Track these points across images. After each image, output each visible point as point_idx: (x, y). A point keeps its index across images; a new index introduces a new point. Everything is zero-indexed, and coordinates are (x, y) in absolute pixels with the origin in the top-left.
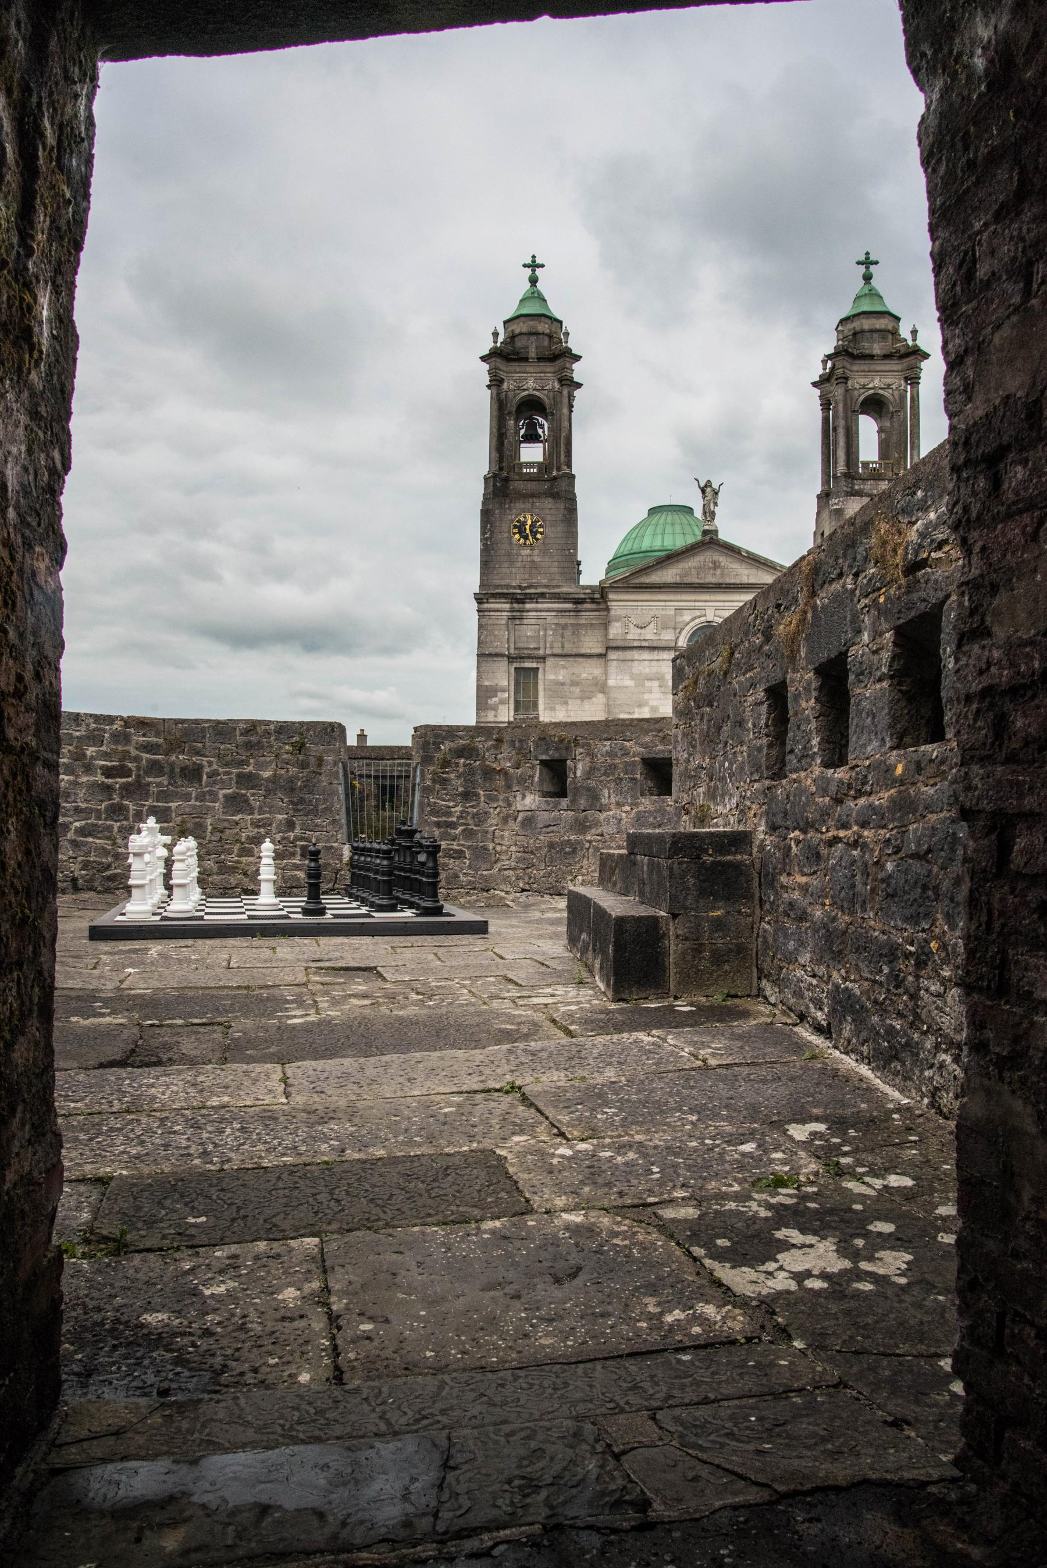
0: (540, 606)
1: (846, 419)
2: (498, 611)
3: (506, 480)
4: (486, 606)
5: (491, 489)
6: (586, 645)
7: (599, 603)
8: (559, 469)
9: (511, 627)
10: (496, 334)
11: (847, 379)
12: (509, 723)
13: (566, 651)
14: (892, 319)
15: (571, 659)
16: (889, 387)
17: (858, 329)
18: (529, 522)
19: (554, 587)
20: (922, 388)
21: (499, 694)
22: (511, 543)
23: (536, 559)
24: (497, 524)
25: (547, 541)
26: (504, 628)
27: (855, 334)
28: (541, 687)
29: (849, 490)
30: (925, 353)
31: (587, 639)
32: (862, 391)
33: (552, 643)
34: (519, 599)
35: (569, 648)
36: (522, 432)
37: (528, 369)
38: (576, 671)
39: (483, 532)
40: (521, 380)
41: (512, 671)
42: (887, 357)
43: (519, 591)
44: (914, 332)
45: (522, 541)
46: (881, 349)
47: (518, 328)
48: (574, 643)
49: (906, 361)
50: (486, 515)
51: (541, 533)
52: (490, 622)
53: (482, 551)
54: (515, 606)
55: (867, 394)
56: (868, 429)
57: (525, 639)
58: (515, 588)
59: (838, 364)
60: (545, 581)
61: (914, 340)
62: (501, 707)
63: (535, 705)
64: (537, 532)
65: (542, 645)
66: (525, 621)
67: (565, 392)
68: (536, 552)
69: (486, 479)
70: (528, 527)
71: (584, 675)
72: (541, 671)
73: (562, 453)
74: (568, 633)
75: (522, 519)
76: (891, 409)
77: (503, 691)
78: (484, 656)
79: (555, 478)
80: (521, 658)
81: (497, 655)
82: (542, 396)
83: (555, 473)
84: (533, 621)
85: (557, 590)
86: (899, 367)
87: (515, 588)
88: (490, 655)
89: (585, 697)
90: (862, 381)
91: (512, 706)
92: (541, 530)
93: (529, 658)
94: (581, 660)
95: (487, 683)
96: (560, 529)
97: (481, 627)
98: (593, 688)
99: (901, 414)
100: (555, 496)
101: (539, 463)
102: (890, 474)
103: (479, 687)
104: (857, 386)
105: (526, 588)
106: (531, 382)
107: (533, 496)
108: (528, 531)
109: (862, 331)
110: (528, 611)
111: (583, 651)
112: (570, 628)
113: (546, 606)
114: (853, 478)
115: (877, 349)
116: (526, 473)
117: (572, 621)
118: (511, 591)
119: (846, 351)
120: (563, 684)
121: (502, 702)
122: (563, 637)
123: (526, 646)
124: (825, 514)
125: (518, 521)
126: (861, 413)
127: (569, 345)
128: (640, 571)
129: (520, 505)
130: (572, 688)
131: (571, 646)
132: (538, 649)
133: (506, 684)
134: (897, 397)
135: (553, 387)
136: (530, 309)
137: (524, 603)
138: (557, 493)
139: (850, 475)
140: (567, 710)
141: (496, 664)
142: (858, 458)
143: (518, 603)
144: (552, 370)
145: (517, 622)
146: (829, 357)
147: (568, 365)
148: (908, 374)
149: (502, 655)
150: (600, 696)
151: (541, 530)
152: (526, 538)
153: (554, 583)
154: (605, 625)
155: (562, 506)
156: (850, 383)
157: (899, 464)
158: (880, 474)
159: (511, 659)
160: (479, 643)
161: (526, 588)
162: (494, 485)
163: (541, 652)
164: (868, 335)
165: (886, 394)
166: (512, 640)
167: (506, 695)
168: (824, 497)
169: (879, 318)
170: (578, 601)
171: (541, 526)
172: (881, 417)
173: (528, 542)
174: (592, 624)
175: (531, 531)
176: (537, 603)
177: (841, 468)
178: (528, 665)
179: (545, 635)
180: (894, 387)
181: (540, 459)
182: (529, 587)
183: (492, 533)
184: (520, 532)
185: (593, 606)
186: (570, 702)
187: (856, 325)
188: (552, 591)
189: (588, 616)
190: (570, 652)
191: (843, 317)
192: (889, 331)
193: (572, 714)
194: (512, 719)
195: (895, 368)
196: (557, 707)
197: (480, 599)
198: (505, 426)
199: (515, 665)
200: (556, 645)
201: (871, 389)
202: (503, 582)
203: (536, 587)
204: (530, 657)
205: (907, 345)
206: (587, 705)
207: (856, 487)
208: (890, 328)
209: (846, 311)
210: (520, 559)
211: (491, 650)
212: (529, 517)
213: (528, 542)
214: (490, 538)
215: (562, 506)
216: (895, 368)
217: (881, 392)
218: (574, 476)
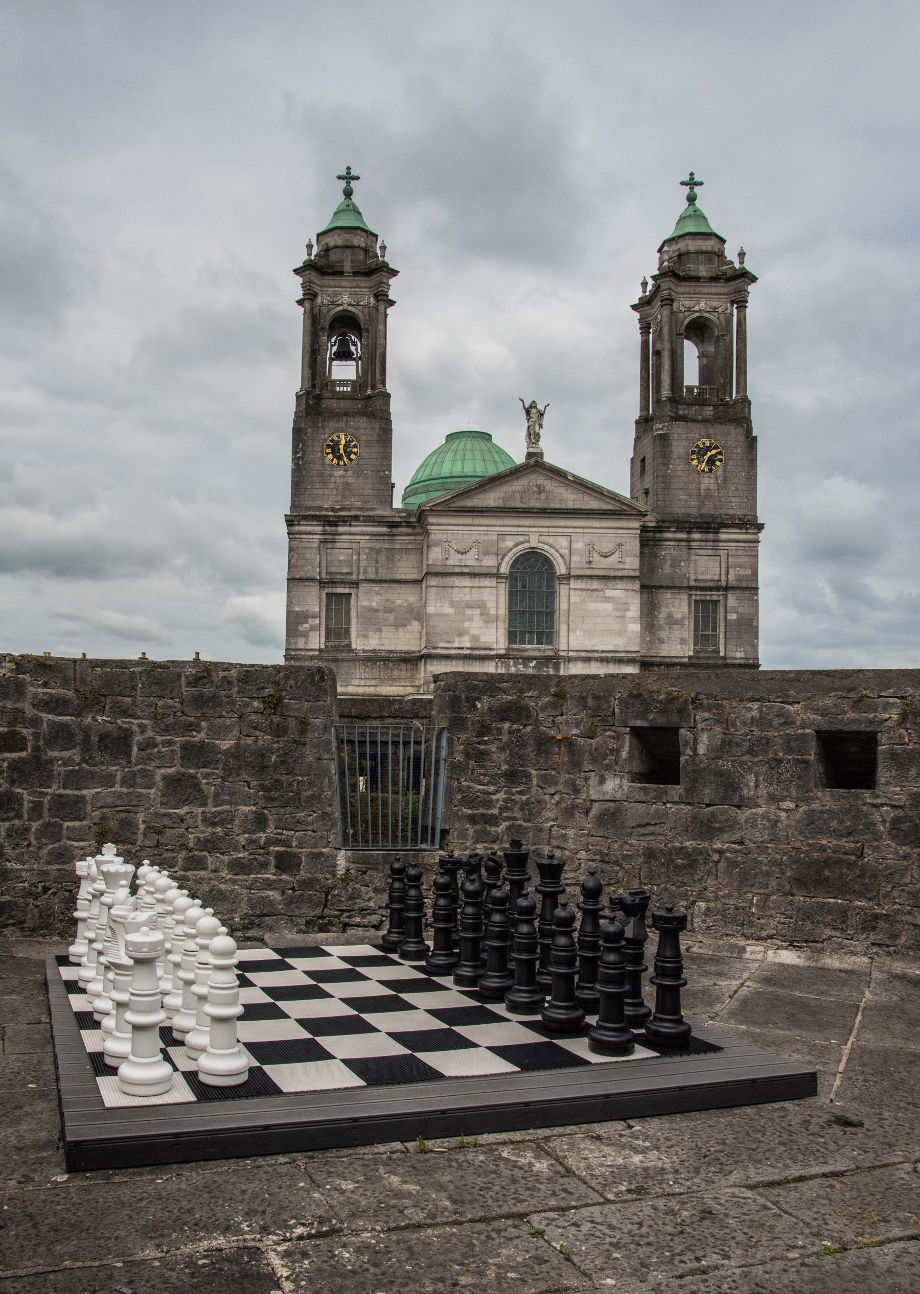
0: (353, 529)
1: (671, 342)
2: (310, 533)
3: (319, 398)
4: (297, 528)
5: (304, 406)
6: (401, 570)
7: (414, 527)
8: (373, 387)
9: (323, 551)
10: (310, 247)
11: (672, 300)
12: (320, 650)
13: (379, 577)
14: (717, 240)
15: (385, 585)
16: (715, 309)
17: (683, 250)
18: (343, 442)
19: (368, 510)
20: (750, 312)
21: (310, 620)
22: (323, 464)
23: (350, 480)
24: (310, 443)
25: (361, 462)
26: (314, 551)
27: (680, 256)
28: (353, 614)
29: (674, 415)
30: (753, 276)
31: (402, 564)
32: (687, 313)
33: (365, 568)
34: (331, 521)
35: (383, 574)
36: (335, 349)
37: (342, 284)
38: (390, 597)
39: (295, 452)
40: (335, 294)
41: (324, 596)
42: (714, 279)
43: (331, 514)
44: (742, 255)
45: (335, 461)
46: (706, 271)
47: (333, 240)
48: (388, 568)
49: (734, 285)
50: (298, 433)
51: (355, 454)
52: (302, 545)
53: (294, 471)
54: (328, 528)
55: (692, 317)
56: (691, 352)
57: (337, 564)
58: (327, 510)
59: (664, 286)
60: (359, 504)
61: (742, 263)
62: (311, 634)
63: (348, 632)
64: (351, 452)
65: (355, 569)
66: (338, 545)
67: (382, 308)
68: (350, 473)
69: (298, 396)
70: (341, 447)
71: (399, 602)
72: (353, 597)
73: (378, 371)
74: (382, 557)
75: (336, 439)
76: (716, 333)
77: (314, 617)
78: (294, 581)
79: (369, 397)
80: (333, 583)
81: (308, 580)
82: (357, 312)
83: (369, 392)
84: (346, 545)
85: (370, 513)
86: (726, 290)
87: (327, 510)
88: (301, 579)
89: (400, 624)
90: (688, 303)
91: (323, 633)
92: (355, 450)
93: (342, 583)
94: (395, 586)
95: (297, 609)
96: (375, 449)
97: (291, 550)
98: (408, 616)
99: (728, 338)
100: (370, 415)
101: (353, 381)
102: (716, 399)
103: (289, 612)
104: (683, 309)
105: (339, 510)
106: (345, 297)
107: (346, 415)
108: (342, 452)
109: (688, 253)
110: (341, 534)
111: (398, 577)
112: (384, 553)
113: (359, 529)
114: (678, 403)
115: (703, 270)
116: (340, 392)
117: (387, 546)
118: (324, 513)
119: (673, 272)
120: (376, 611)
121: (313, 629)
122: (377, 562)
123: (338, 570)
124: (647, 440)
125: (331, 441)
126: (687, 338)
127: (386, 259)
128: (458, 495)
129: (333, 424)
130: (386, 615)
131: (385, 571)
132: (350, 574)
133: (318, 610)
134: (723, 321)
135: (369, 303)
136: (347, 221)
137: (336, 526)
138: (371, 412)
139: (675, 400)
140: (380, 638)
141: (307, 589)
142: (682, 383)
143: (331, 526)
144: (368, 284)
145: (329, 545)
146: (654, 278)
147: (384, 280)
148: (734, 297)
149: (314, 580)
150: (415, 624)
151: (355, 450)
152: (340, 458)
153: (369, 506)
154: (420, 552)
155: (377, 426)
156: (675, 304)
157: (724, 388)
158: (705, 400)
159: (322, 584)
160: (289, 567)
161: (339, 510)
162: (307, 403)
163: (354, 577)
164: (694, 257)
165: (712, 317)
166: (324, 564)
167: (318, 621)
168: (644, 423)
169: (706, 239)
170: (393, 525)
171: (355, 446)
172: (702, 341)
173: (341, 463)
174: (407, 549)
175: (345, 451)
176: (350, 526)
177: (666, 392)
178: (340, 590)
179: (358, 560)
180: (720, 310)
181: (354, 378)
182: (342, 509)
183: (304, 452)
184: (333, 453)
185: (409, 530)
186: (384, 629)
187: (681, 246)
188: (367, 514)
189: (403, 540)
190: (384, 578)
191: (666, 238)
192: (715, 253)
193: (386, 642)
194: (323, 647)
195: (722, 290)
196: (370, 634)
197: (290, 522)
198: (318, 343)
199: (327, 590)
200: (369, 570)
201: (696, 311)
202: (315, 504)
203: (349, 510)
204: (343, 583)
205: (734, 267)
206: (401, 632)
207: (681, 412)
208: (716, 250)
209: (669, 233)
210: (333, 480)
211: (302, 574)
212: (342, 436)
213: (341, 463)
214: (302, 458)
215: (377, 426)
216: (722, 290)
217: (707, 315)
218: (389, 396)
